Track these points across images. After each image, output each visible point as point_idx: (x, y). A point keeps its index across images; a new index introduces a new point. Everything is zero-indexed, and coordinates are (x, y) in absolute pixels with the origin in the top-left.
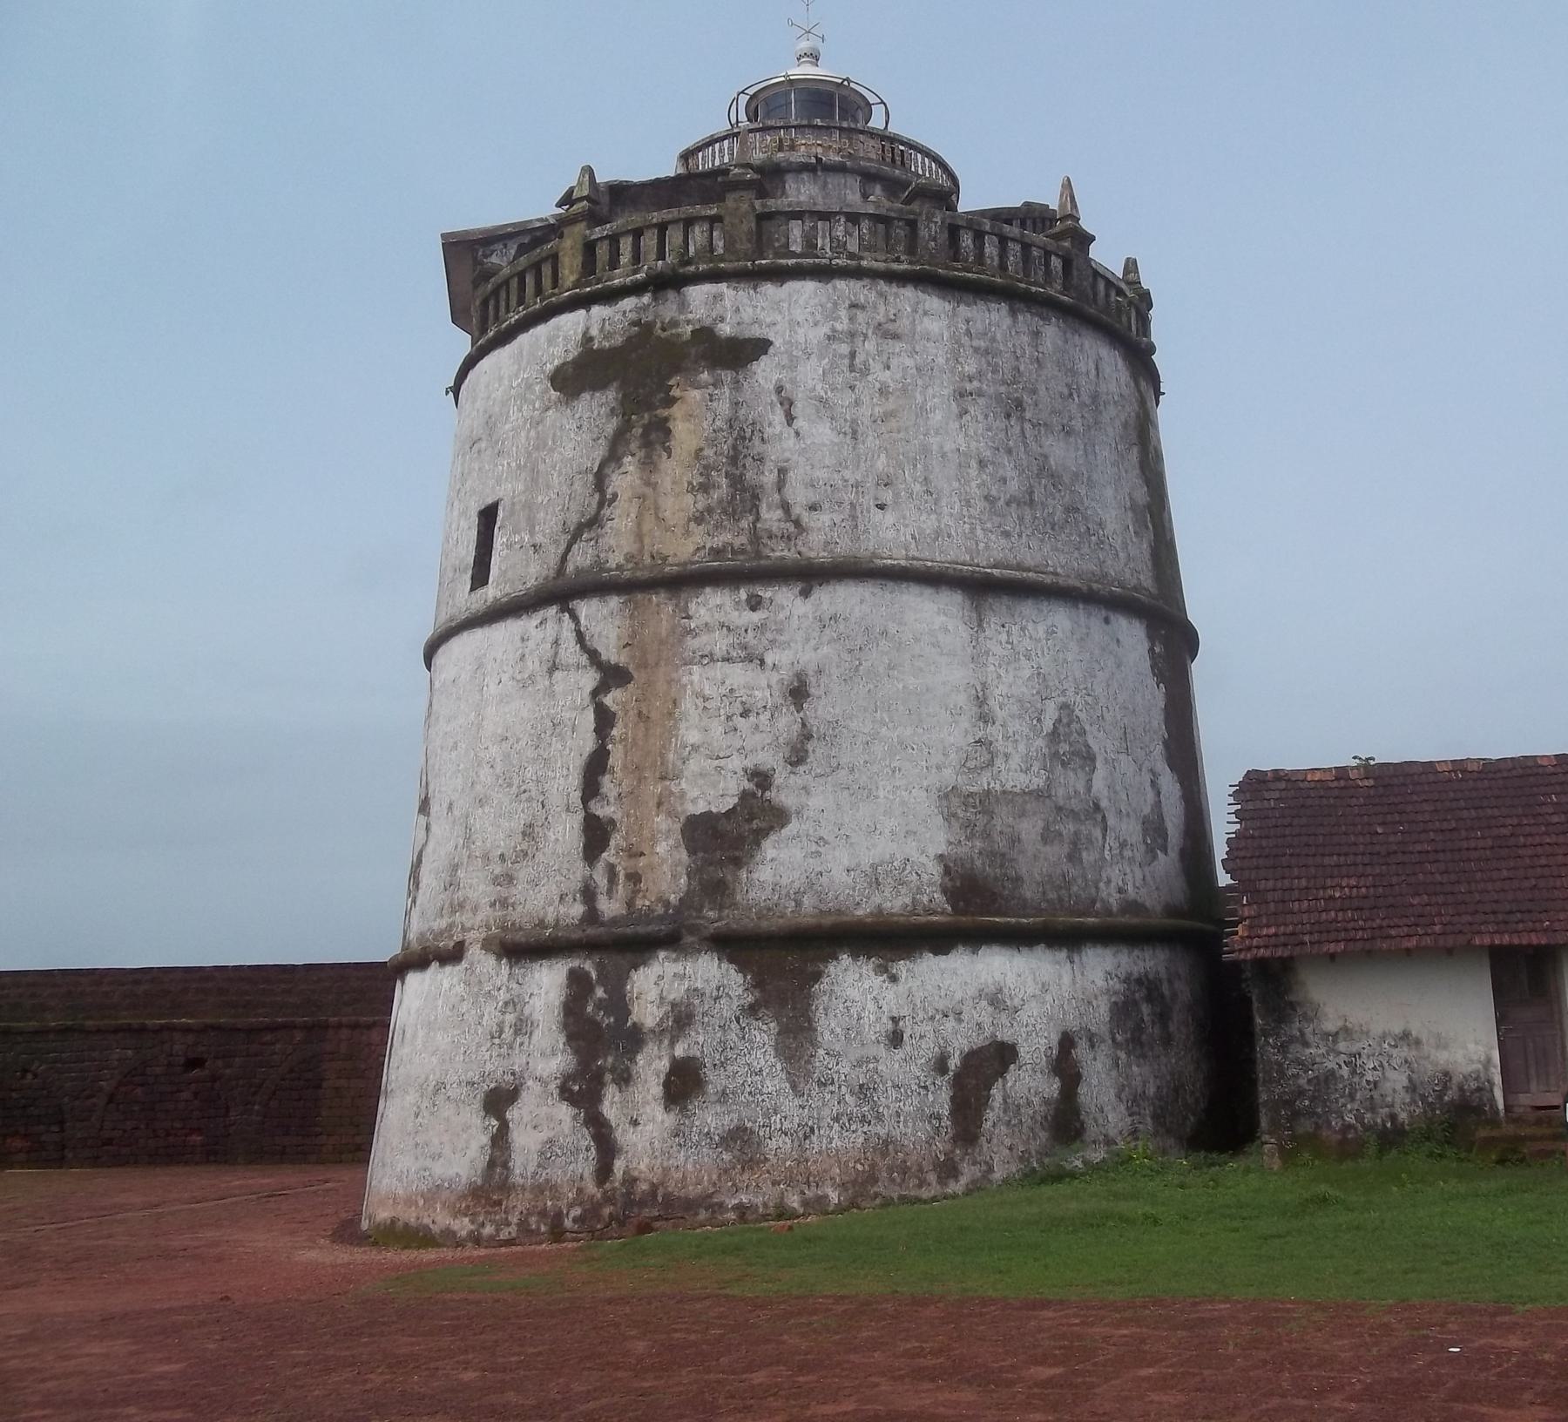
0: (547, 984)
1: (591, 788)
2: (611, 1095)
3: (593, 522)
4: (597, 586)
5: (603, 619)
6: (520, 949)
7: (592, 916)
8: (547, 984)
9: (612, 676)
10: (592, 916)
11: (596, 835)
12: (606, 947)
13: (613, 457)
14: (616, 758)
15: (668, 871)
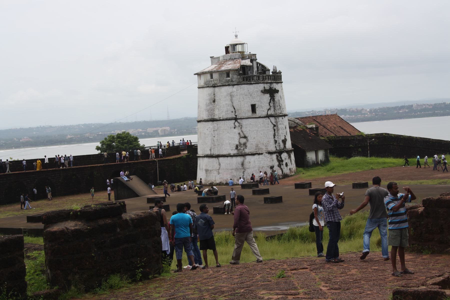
0: (274, 156)
1: (274, 137)
2: (282, 166)
3: (270, 109)
4: (272, 116)
5: (273, 119)
6: (270, 153)
7: (277, 149)
8: (274, 156)
9: (275, 126)
10: (277, 149)
11: (276, 142)
12: (279, 153)
13: (270, 102)
14: (276, 134)
15: (282, 146)
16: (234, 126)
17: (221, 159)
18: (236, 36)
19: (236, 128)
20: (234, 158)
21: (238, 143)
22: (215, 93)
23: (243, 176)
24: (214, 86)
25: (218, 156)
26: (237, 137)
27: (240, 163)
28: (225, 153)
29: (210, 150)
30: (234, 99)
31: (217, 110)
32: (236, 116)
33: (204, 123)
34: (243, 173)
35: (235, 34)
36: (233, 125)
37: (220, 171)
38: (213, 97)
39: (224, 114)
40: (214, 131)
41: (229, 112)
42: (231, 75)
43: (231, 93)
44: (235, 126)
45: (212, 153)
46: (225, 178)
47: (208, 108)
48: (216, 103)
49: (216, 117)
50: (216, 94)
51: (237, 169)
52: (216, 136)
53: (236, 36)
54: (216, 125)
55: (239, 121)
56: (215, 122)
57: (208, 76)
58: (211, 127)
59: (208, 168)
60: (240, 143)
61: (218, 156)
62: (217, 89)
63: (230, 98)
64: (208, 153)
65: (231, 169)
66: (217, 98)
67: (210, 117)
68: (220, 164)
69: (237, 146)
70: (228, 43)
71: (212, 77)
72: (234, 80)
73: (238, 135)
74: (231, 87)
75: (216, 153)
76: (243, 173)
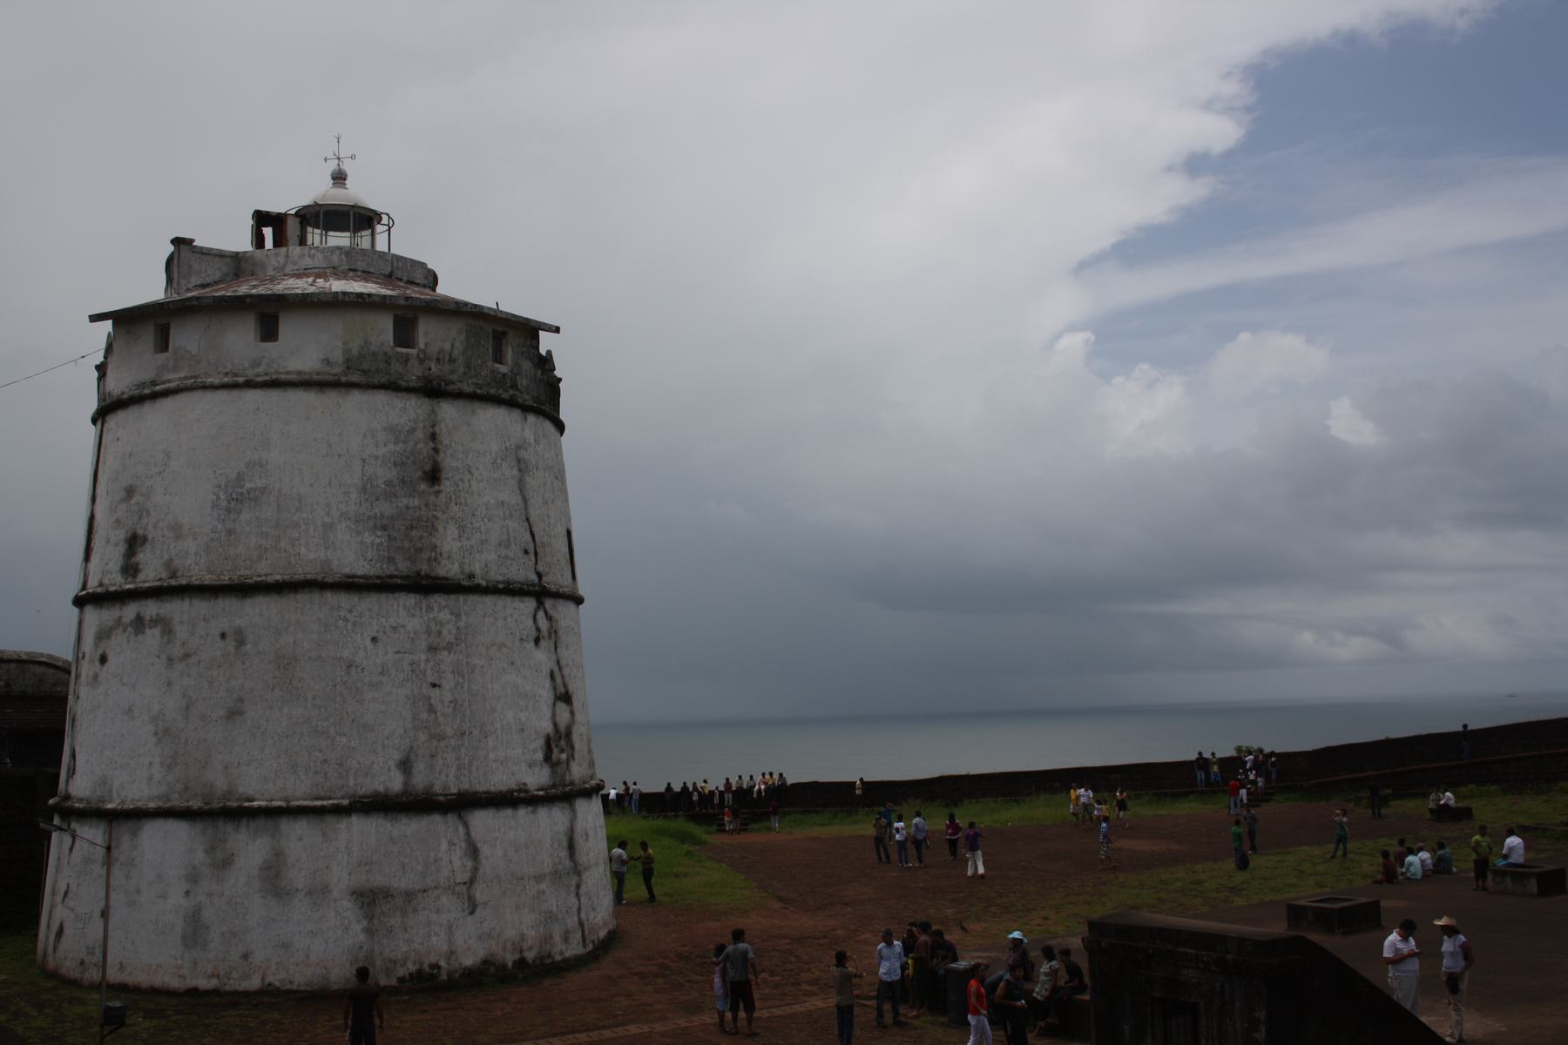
16: (534, 634)
17: (481, 820)
18: (339, 178)
19: (543, 643)
20: (543, 812)
21: (547, 727)
22: (442, 429)
23: (579, 910)
24: (433, 390)
25: (463, 804)
26: (546, 694)
27: (565, 844)
28: (499, 781)
29: (405, 765)
30: (531, 481)
31: (452, 531)
32: (539, 575)
33: (344, 600)
34: (578, 895)
35: (332, 166)
36: (530, 622)
37: (480, 894)
38: (425, 449)
39: (491, 556)
40: (433, 649)
41: (515, 550)
42: (509, 354)
43: (518, 447)
44: (538, 630)
45: (420, 780)
46: (510, 934)
47: (386, 508)
48: (446, 486)
49: (449, 569)
50: (445, 439)
51: (556, 876)
52: (448, 683)
53: (339, 178)
54: (444, 616)
55: (548, 603)
56: (438, 600)
57: (382, 329)
58: (414, 624)
59: (379, 880)
60: (555, 725)
61: (463, 804)
62: (449, 411)
63: (515, 471)
64: (394, 783)
65: (539, 878)
66: (449, 462)
67: (403, 566)
68: (473, 852)
69: (548, 741)
70: (285, 202)
71: (404, 332)
72: (523, 382)
73: (548, 683)
74: (516, 414)
75: (447, 780)
76: (578, 895)
